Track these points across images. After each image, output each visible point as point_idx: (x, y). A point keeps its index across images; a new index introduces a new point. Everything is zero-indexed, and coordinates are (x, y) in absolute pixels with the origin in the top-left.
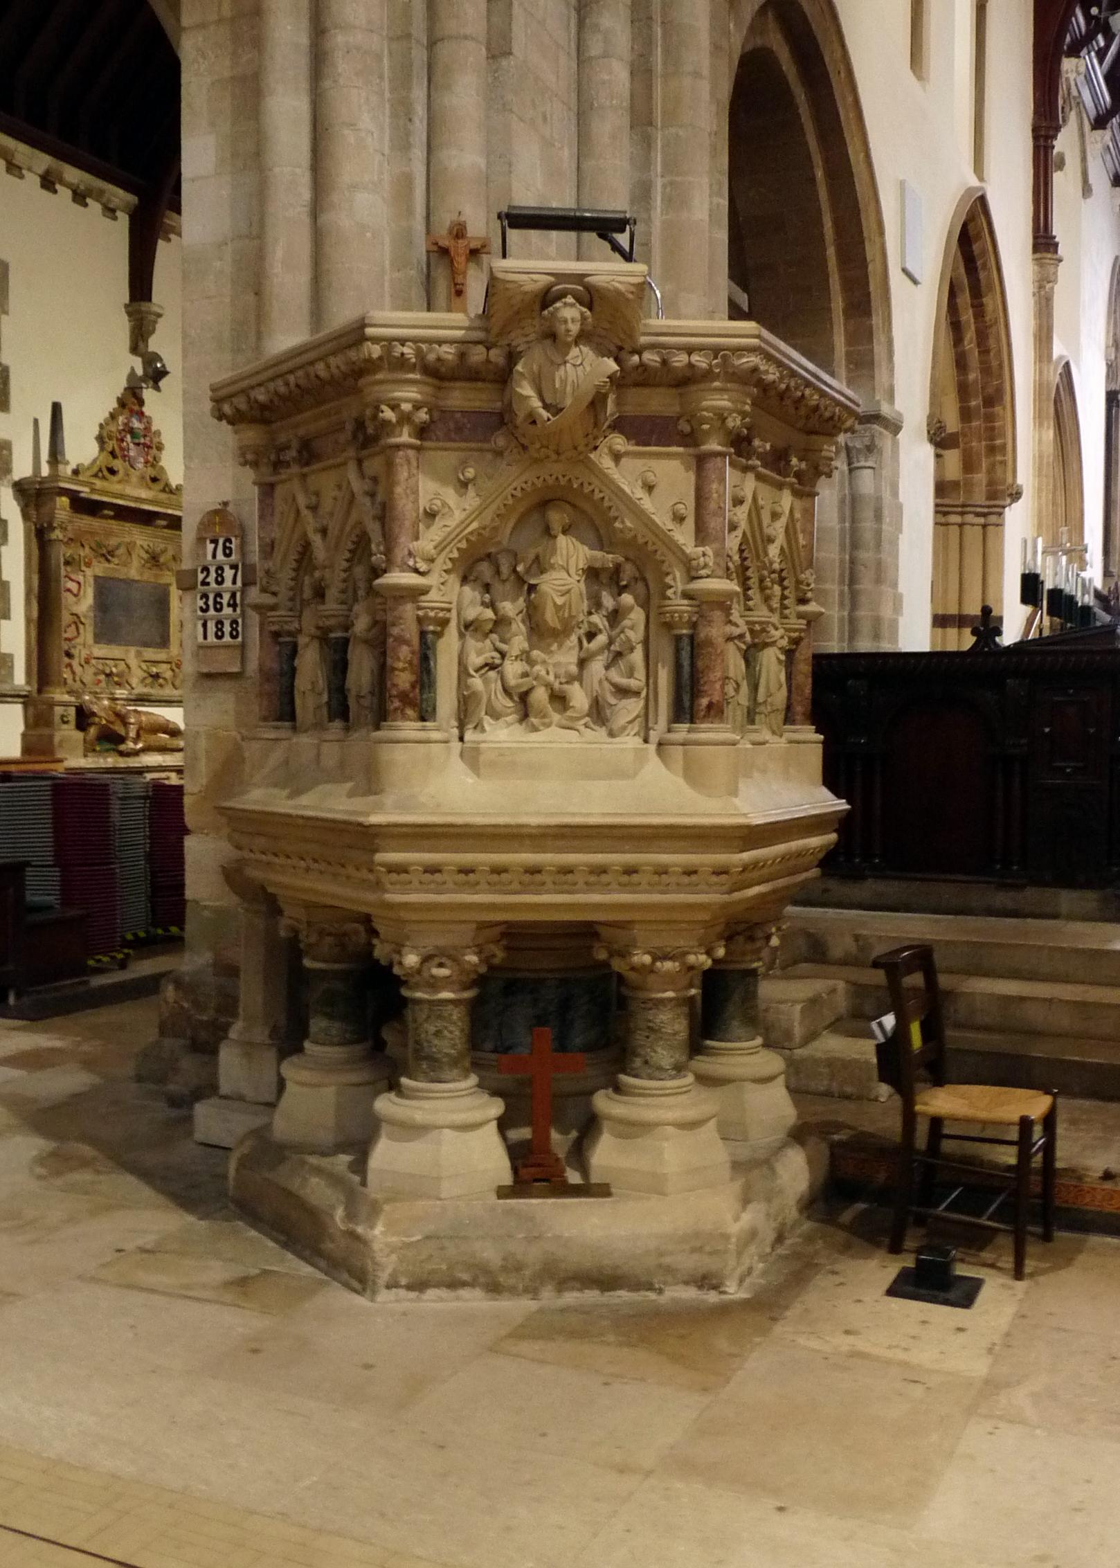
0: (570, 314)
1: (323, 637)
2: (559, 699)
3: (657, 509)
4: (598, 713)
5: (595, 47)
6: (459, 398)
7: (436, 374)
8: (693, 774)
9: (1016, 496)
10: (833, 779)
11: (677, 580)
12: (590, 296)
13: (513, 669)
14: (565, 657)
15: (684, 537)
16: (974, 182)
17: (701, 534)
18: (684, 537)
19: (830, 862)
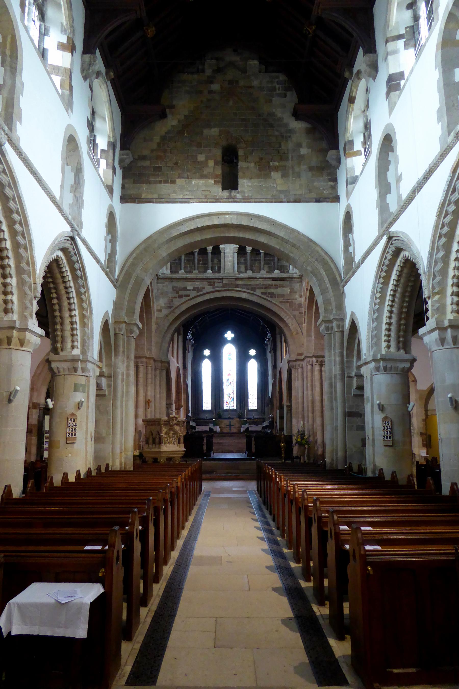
0: (174, 419)
1: (153, 438)
2: (171, 442)
3: (177, 429)
4: (174, 443)
5: (157, 380)
6: (166, 423)
7: (165, 421)
8: (180, 447)
9: (182, 407)
10: (185, 448)
11: (178, 434)
12: (175, 417)
13: (168, 440)
14: (171, 439)
15: (179, 431)
16: (178, 365)
17: (180, 431)
18: (179, 431)
19: (185, 454)
